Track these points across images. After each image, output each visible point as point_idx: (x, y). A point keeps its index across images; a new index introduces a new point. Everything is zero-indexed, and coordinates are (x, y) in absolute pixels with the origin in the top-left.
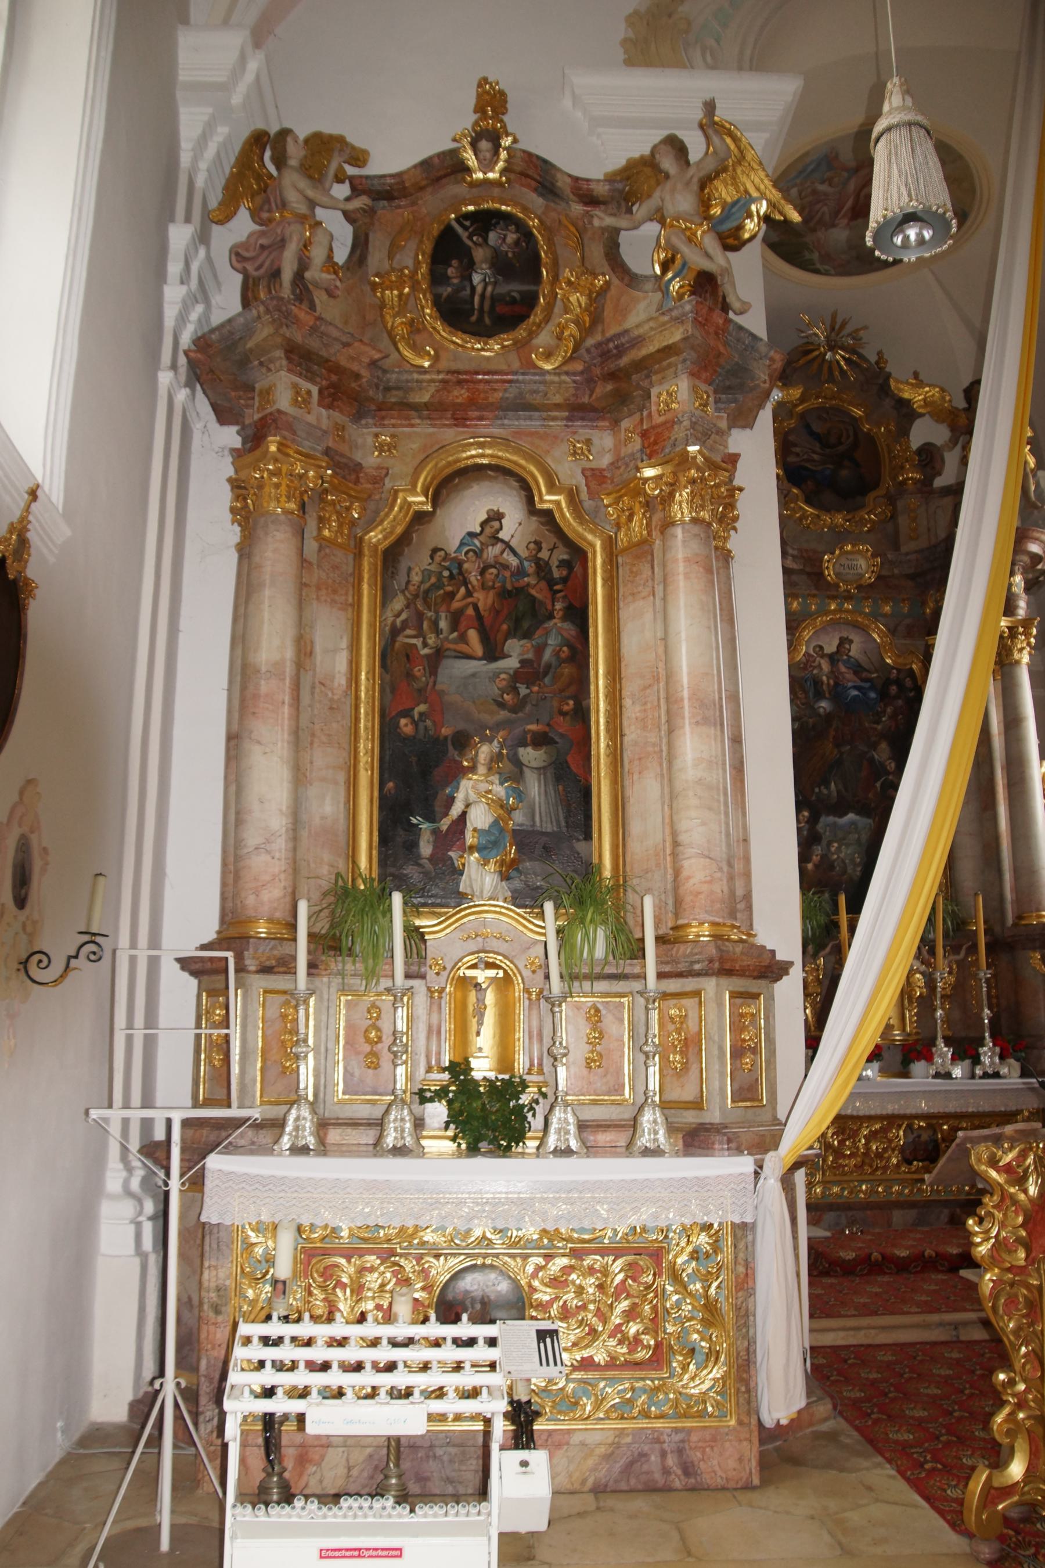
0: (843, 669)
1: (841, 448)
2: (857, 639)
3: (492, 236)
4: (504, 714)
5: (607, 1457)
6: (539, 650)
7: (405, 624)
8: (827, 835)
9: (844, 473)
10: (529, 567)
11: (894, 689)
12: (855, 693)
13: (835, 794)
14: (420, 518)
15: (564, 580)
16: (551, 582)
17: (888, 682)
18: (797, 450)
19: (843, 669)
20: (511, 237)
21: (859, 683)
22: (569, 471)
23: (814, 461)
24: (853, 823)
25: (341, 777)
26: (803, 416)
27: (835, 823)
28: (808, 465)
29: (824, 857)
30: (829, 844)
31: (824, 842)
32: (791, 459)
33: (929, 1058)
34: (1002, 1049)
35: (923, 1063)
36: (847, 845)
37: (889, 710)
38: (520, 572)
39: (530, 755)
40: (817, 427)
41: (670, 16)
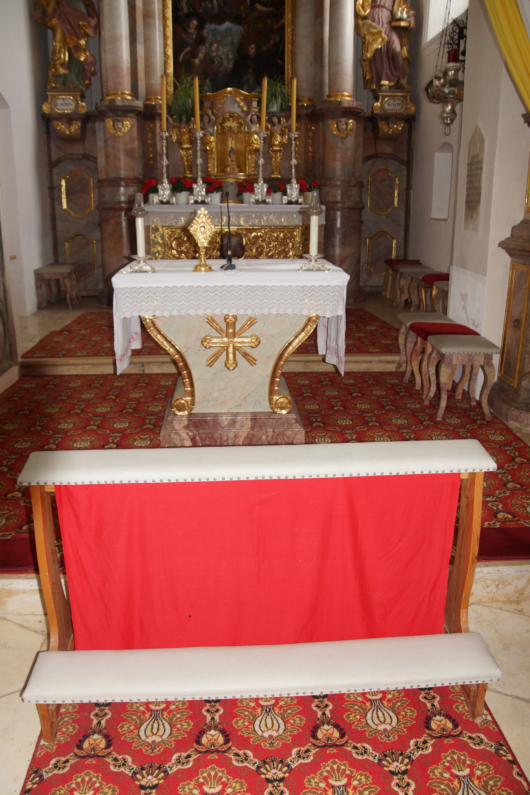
8: (210, 38)
13: (216, 7)
24: (229, 29)
27: (216, 29)
29: (207, 54)
30: (211, 45)
31: (207, 44)
34: (301, 186)
35: (248, 193)
36: (224, 46)
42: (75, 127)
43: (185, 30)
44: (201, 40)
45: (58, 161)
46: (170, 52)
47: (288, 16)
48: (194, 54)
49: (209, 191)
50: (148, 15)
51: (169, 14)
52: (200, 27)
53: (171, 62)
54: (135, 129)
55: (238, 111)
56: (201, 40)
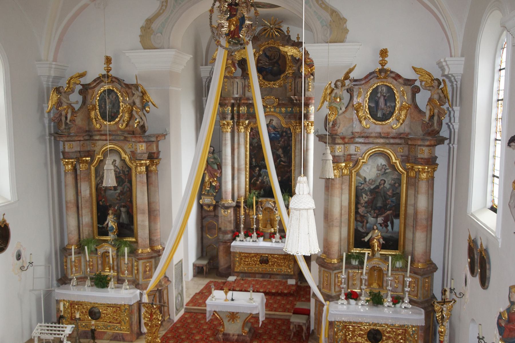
0: (270, 128)
1: (275, 60)
2: (275, 119)
3: (110, 96)
4: (118, 201)
5: (112, 336)
6: (123, 188)
7: (100, 183)
9: (275, 68)
10: (121, 172)
11: (284, 134)
12: (273, 135)
14: (101, 161)
15: (128, 175)
16: (125, 175)
17: (283, 132)
18: (261, 62)
19: (270, 128)
20: (114, 97)
21: (275, 132)
22: (128, 151)
23: (266, 65)
25: (89, 214)
26: (264, 51)
28: (264, 66)
29: (262, 180)
30: (264, 177)
32: (259, 65)
33: (274, 237)
37: (283, 140)
38: (120, 173)
39: (123, 209)
40: (268, 54)
41: (149, 29)
42: (212, 208)
43: (254, 172)
44: (260, 175)
45: (205, 217)
46: (247, 180)
47: (293, 168)
48: (257, 180)
49: (258, 237)
50: (239, 170)
51: (248, 166)
52: (260, 170)
53: (248, 183)
54: (232, 213)
55: (270, 206)
56: (260, 175)
